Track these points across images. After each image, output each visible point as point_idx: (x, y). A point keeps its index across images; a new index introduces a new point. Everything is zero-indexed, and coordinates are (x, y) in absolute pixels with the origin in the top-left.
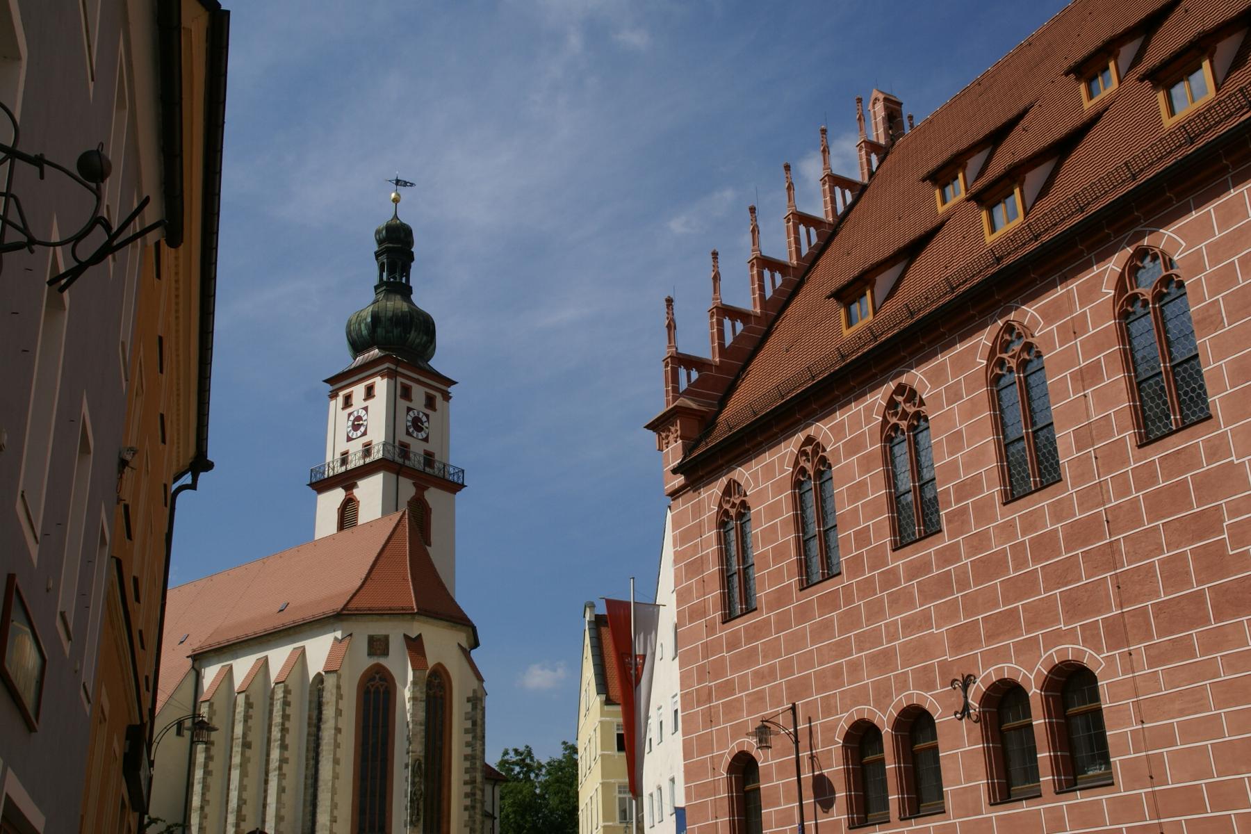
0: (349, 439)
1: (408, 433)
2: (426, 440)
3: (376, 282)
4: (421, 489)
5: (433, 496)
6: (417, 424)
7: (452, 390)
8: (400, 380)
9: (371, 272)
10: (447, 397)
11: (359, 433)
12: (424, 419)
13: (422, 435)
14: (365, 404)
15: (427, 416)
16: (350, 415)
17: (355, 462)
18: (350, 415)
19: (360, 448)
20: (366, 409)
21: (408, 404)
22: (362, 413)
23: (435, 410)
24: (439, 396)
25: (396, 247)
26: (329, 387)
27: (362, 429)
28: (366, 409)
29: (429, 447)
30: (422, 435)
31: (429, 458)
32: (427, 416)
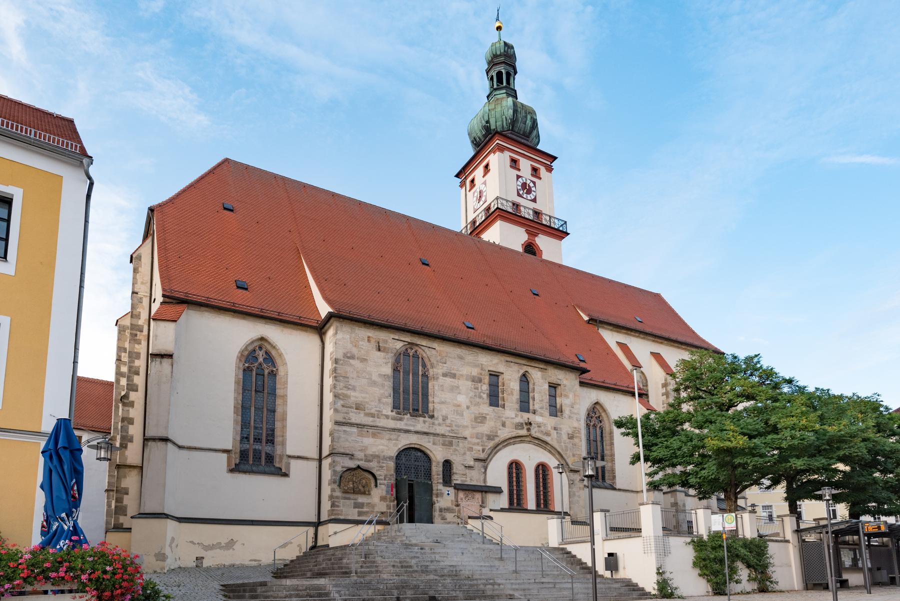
1: (519, 195)
2: (534, 200)
4: (532, 234)
5: (543, 242)
6: (526, 188)
10: (550, 169)
11: (481, 203)
12: (532, 185)
13: (531, 196)
15: (534, 183)
21: (516, 172)
23: (540, 178)
27: (483, 199)
28: (485, 183)
29: (538, 206)
30: (531, 196)
31: (537, 213)
32: (534, 183)
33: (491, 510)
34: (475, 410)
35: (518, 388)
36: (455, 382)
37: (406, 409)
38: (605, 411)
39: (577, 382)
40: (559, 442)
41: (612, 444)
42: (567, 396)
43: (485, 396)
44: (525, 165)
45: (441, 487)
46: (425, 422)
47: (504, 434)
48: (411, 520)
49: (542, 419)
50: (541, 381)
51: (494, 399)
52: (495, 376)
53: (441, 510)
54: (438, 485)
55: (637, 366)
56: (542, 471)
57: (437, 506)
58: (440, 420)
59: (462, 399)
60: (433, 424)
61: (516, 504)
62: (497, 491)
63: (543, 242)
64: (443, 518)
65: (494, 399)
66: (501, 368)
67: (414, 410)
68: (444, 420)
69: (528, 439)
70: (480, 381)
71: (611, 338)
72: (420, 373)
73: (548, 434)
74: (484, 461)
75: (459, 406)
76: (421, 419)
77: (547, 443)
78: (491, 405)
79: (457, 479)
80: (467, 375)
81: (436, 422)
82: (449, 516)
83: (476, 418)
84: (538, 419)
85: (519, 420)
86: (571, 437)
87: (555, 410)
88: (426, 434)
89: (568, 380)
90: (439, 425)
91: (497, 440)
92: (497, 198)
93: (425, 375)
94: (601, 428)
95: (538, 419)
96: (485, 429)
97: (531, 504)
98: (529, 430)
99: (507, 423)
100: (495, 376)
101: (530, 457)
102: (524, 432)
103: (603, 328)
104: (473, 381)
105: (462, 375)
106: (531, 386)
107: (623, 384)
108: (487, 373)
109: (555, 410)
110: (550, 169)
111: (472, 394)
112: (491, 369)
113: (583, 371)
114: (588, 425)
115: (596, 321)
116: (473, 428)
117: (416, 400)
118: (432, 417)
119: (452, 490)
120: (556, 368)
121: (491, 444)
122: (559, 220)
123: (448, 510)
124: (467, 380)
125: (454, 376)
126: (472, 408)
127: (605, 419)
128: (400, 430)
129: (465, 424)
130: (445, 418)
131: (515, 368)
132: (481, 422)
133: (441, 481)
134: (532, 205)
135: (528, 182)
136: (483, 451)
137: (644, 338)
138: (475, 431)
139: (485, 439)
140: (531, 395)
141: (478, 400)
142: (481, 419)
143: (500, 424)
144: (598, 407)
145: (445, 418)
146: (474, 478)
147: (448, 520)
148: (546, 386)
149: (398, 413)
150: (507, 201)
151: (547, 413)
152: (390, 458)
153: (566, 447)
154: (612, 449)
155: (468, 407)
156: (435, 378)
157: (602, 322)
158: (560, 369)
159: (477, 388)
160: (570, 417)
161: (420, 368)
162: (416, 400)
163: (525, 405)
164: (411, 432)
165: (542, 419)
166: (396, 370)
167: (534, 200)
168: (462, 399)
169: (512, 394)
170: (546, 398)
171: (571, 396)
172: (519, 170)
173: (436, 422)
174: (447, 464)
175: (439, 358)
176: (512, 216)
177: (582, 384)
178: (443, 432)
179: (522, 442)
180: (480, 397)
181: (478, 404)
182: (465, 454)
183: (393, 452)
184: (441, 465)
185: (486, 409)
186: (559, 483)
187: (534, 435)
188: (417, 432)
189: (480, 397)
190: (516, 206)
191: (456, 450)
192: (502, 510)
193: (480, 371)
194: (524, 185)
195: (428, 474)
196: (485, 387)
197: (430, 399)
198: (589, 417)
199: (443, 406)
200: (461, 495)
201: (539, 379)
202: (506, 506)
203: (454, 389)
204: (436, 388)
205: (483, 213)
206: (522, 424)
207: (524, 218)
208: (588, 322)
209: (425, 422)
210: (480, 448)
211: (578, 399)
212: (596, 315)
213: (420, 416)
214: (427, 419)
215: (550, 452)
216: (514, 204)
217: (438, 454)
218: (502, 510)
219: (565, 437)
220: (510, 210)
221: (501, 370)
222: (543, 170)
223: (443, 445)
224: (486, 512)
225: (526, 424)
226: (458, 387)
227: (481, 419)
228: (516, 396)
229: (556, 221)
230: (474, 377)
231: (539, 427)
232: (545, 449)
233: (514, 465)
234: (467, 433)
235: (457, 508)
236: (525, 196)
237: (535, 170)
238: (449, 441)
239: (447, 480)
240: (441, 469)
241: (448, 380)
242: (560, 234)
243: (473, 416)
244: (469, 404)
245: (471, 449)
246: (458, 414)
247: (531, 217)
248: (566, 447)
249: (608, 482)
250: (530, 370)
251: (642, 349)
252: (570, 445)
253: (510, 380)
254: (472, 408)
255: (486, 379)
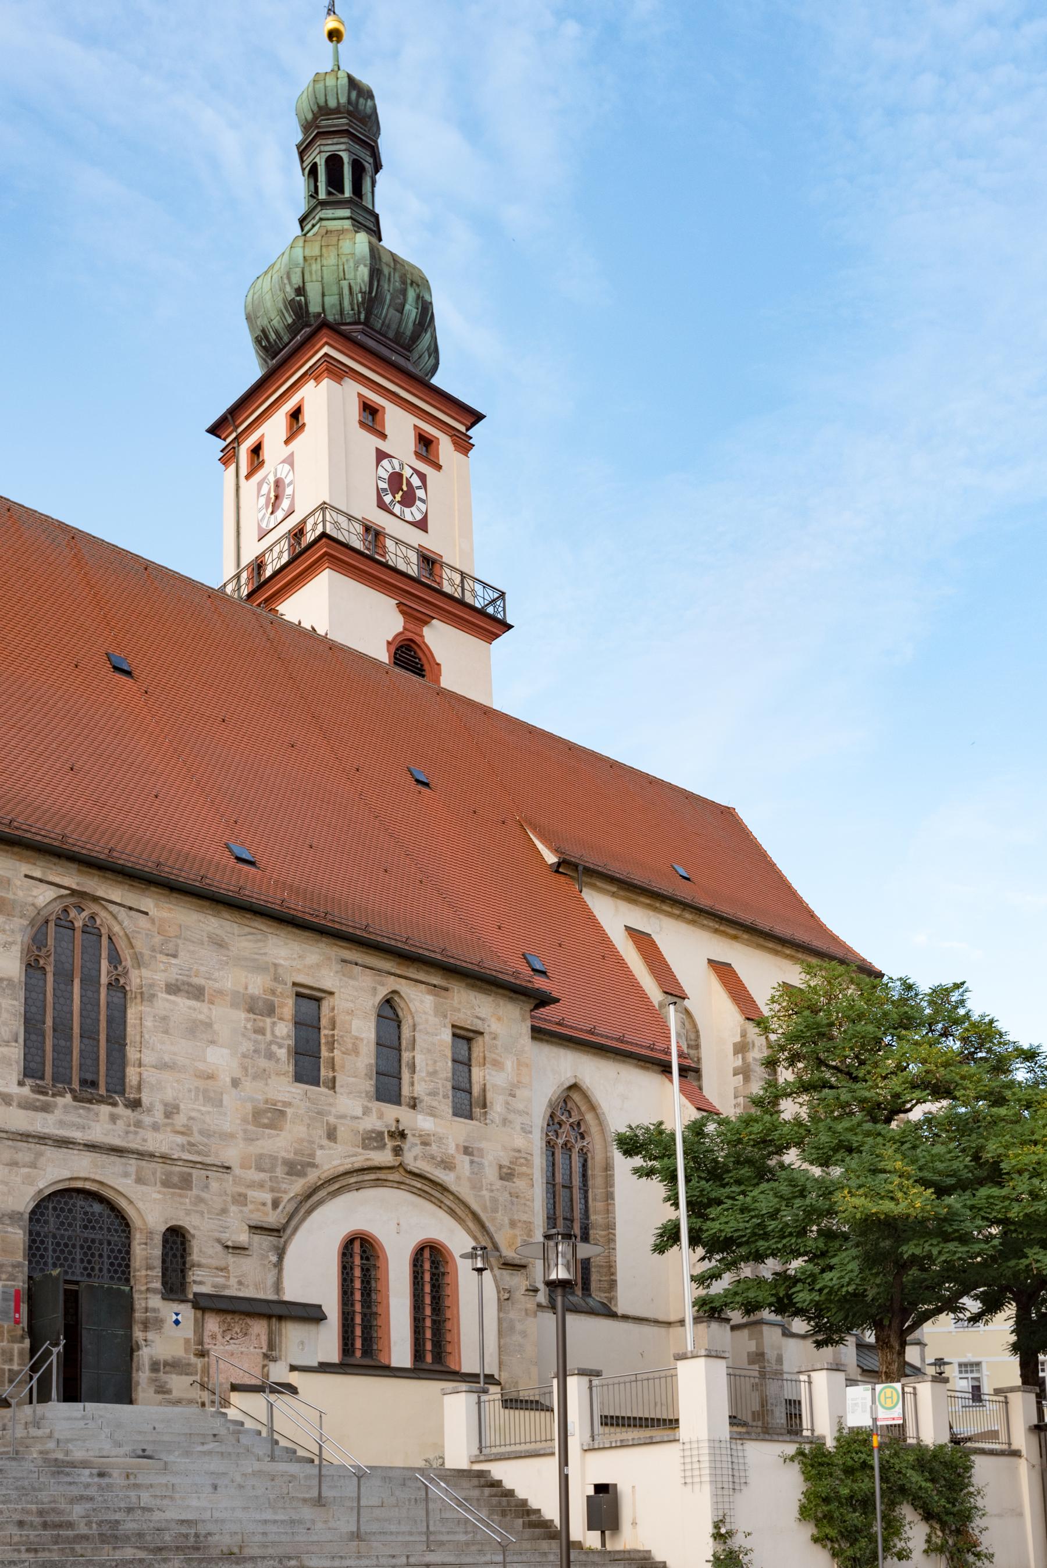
1: (381, 505)
2: (422, 525)
5: (441, 639)
6: (400, 490)
10: (464, 445)
12: (416, 481)
13: (413, 514)
14: (287, 450)
15: (422, 477)
16: (260, 485)
18: (260, 485)
21: (374, 442)
23: (438, 467)
24: (445, 446)
30: (413, 514)
32: (422, 477)
33: (293, 1368)
34: (255, 1091)
35: (372, 1036)
36: (201, 1010)
37: (61, 1078)
38: (593, 1107)
39: (525, 1029)
40: (476, 1187)
41: (609, 1196)
42: (497, 1064)
43: (282, 1053)
45: (156, 1301)
46: (113, 1118)
47: (333, 1159)
48: (71, 1395)
49: (433, 1124)
50: (433, 1020)
51: (308, 1062)
52: (310, 998)
53: (155, 1367)
54: (148, 1296)
55: (675, 993)
56: (430, 1263)
57: (145, 1355)
58: (158, 1115)
59: (221, 1059)
60: (138, 1124)
61: (360, 1352)
62: (312, 1315)
63: (441, 639)
64: (162, 1390)
65: (308, 1062)
66: (327, 978)
67: (83, 1082)
68: (168, 1115)
69: (395, 1176)
70: (270, 1010)
71: (613, 916)
72: (104, 980)
73: (447, 1165)
74: (278, 1234)
75: (211, 1077)
76: (105, 1109)
77: (444, 1189)
78: (299, 1078)
79: (202, 1281)
80: (235, 993)
81: (147, 1120)
82: (179, 1384)
83: (257, 1114)
84: (421, 1122)
86: (507, 1175)
87: (467, 1102)
88: (118, 1151)
89: (503, 1022)
90: (155, 1127)
91: (313, 1177)
92: (323, 507)
93: (117, 987)
94: (584, 1154)
96: (281, 1144)
97: (400, 1349)
98: (398, 1151)
99: (342, 1132)
100: (310, 998)
101: (400, 1224)
102: (384, 1157)
103: (593, 886)
104: (251, 1010)
105: (220, 992)
106: (406, 1032)
107: (640, 1039)
108: (290, 991)
109: (467, 1102)
110: (464, 445)
111: (246, 1046)
112: (301, 979)
113: (542, 1000)
114: (550, 1145)
115: (575, 866)
116: (250, 1140)
117: (90, 1056)
118: (135, 1104)
119: (186, 1312)
120: (473, 987)
121: (297, 1186)
122: (485, 585)
123: (175, 1366)
124: (234, 1005)
125: (197, 993)
126: (247, 1084)
127: (594, 1129)
128: (42, 1139)
129: (227, 1127)
130: (171, 1111)
131: (365, 980)
132: (271, 1126)
133: (157, 1285)
134: (415, 537)
135: (407, 472)
136: (275, 1204)
137: (692, 922)
138: (255, 1149)
139: (280, 1171)
140: (406, 1056)
141: (263, 1063)
142: (270, 1116)
143: (319, 1133)
144: (576, 1096)
145: (171, 1111)
146: (248, 1279)
147: (176, 1394)
148: (447, 1036)
149: (40, 1090)
150: (350, 518)
152: (14, 1217)
153: (494, 1200)
154: (609, 1210)
155: (235, 1083)
156: (147, 996)
157: (590, 872)
158: (481, 990)
159: (261, 1031)
160: (505, 1122)
161: (104, 964)
162: (90, 1056)
163: (388, 1085)
164: (75, 1145)
165: (433, 1124)
166: (33, 966)
167: (422, 525)
168: (221, 1059)
169: (356, 1051)
170: (446, 1066)
171: (509, 1064)
172: (383, 436)
173: (147, 1120)
174: (176, 1240)
175: (157, 939)
176: (362, 561)
177: (539, 1034)
178: (164, 1149)
179: (379, 1183)
180: (270, 1056)
181: (262, 1075)
182: (224, 1211)
183: (23, 1201)
184: (158, 1240)
185: (285, 1089)
186: (473, 1293)
187: (413, 1165)
188: (92, 1147)
189: (270, 1056)
190: (374, 533)
191: (200, 1200)
192: (324, 1368)
193: (270, 984)
194: (396, 480)
195: (122, 1265)
196: (284, 1029)
197: (132, 1053)
198: (553, 1122)
199: (166, 1075)
200: (213, 1324)
201: (430, 1014)
202: (334, 1356)
203: (198, 1029)
204: (148, 1023)
205: (285, 545)
206: (380, 1134)
207: (395, 570)
208: (557, 868)
209: (113, 1118)
210: (268, 1197)
211: (525, 1074)
212: (575, 853)
213: (101, 1100)
214: (121, 1110)
215: (452, 1213)
216: (367, 529)
217: (150, 1210)
218: (324, 1368)
219: (491, 1174)
220: (358, 544)
221: (327, 984)
222: (445, 446)
223: (166, 1183)
224: (279, 1373)
225: (391, 1135)
226: (209, 1025)
227: (270, 1116)
228: (366, 1057)
229: (478, 588)
230: (253, 998)
231: (425, 1144)
232: (440, 1204)
233: (357, 1247)
234: (231, 1154)
235: (199, 1362)
236: (397, 509)
237: (425, 442)
238: (182, 1173)
239: (175, 1280)
240: (158, 1252)
241: (183, 1003)
242: (488, 624)
243: (249, 1107)
244: (238, 1073)
245: (241, 1199)
246: (208, 1099)
247: (413, 570)
248: (494, 1200)
249: (598, 1296)
250: (406, 989)
251: (689, 949)
252: (503, 1198)
253: (351, 1013)
254: (247, 1084)
255: (288, 1007)
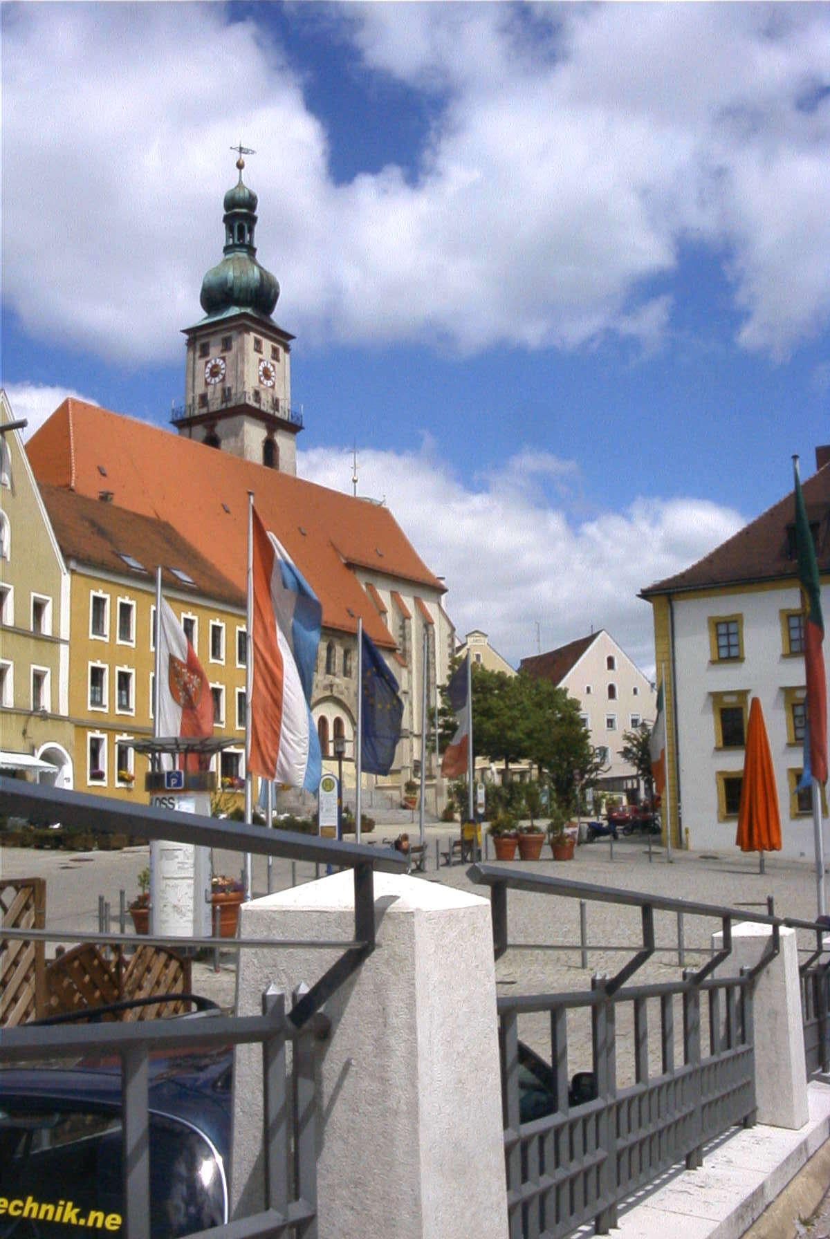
0: (207, 384)
2: (273, 387)
3: (224, 244)
6: (266, 374)
7: (291, 343)
8: (253, 335)
9: (219, 235)
13: (270, 383)
17: (216, 405)
19: (219, 394)
20: (223, 359)
22: (220, 362)
24: (281, 350)
25: (240, 215)
26: (186, 337)
31: (276, 404)
44: (267, 345)
49: (339, 681)
56: (338, 723)
73: (342, 693)
84: (337, 681)
85: (326, 682)
95: (337, 681)
102: (328, 693)
109: (347, 672)
110: (287, 349)
151: (342, 674)
237: (275, 351)
